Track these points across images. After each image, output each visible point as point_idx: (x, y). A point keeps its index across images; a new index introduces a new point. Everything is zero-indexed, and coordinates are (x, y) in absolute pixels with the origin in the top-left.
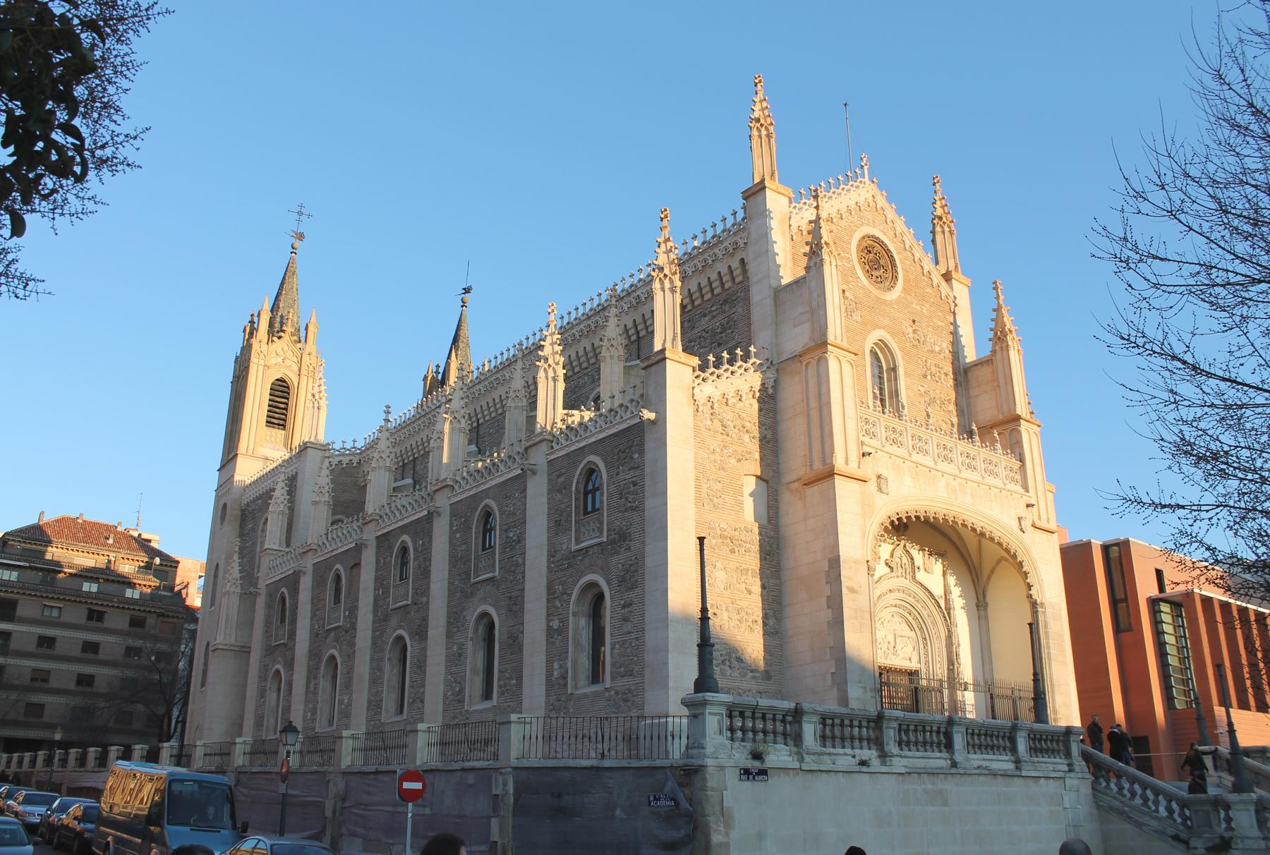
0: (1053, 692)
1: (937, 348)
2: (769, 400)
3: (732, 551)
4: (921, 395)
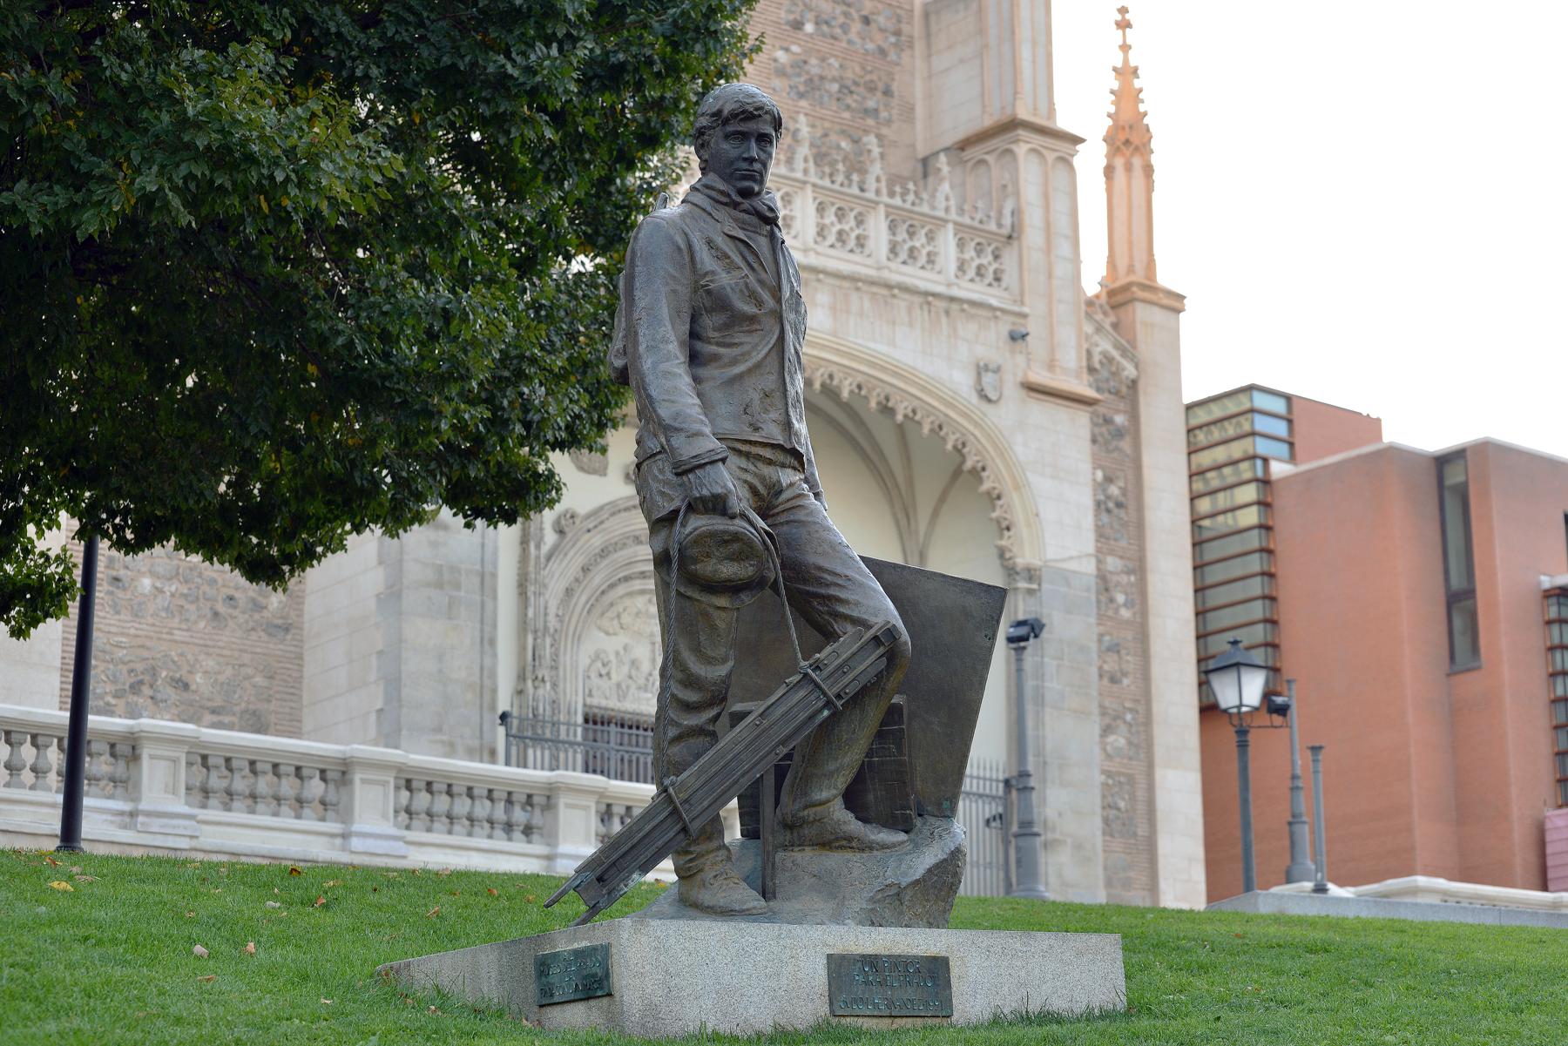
4: (781, 72)
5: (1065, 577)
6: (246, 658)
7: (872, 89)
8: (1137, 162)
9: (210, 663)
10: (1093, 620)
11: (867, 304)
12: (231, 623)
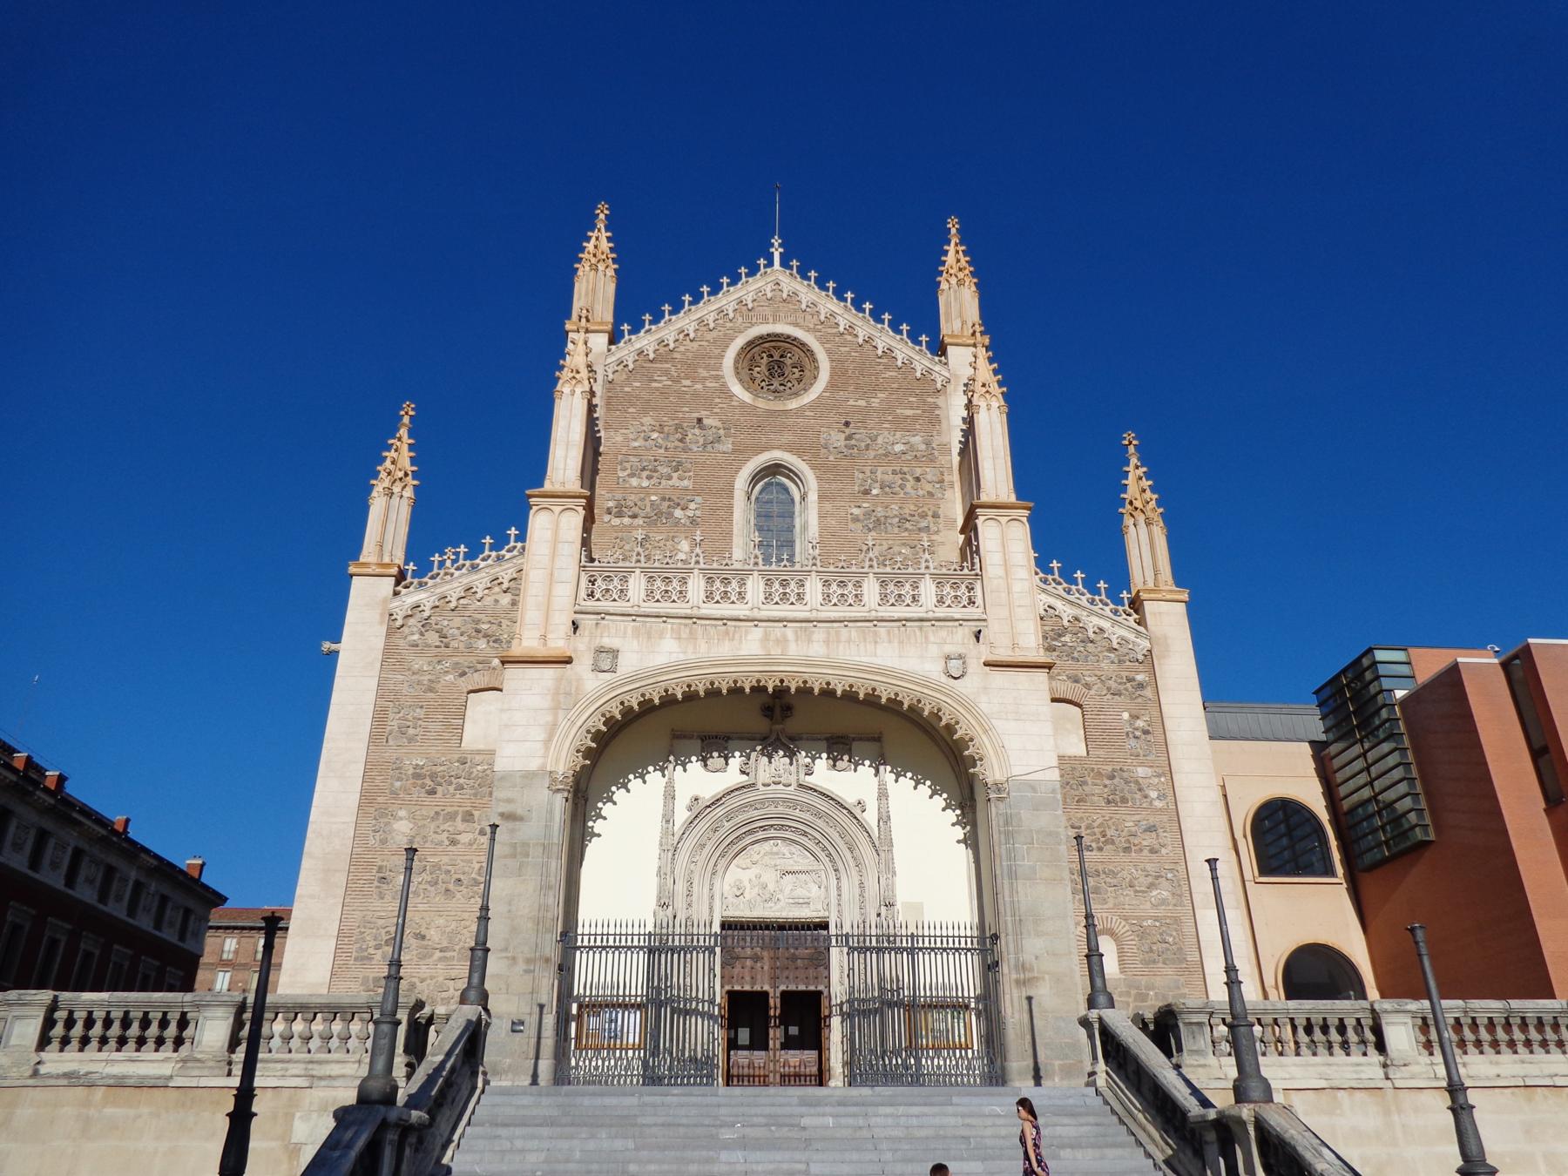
0: (1019, 934)
1: (898, 448)
3: (432, 792)
5: (1032, 787)
6: (466, 915)
7: (924, 516)
8: (1141, 518)
9: (441, 921)
10: (1060, 812)
11: (854, 633)
12: (458, 895)
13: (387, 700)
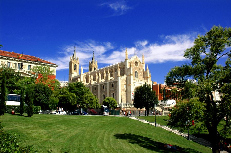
2: (127, 79)
13: (121, 85)
